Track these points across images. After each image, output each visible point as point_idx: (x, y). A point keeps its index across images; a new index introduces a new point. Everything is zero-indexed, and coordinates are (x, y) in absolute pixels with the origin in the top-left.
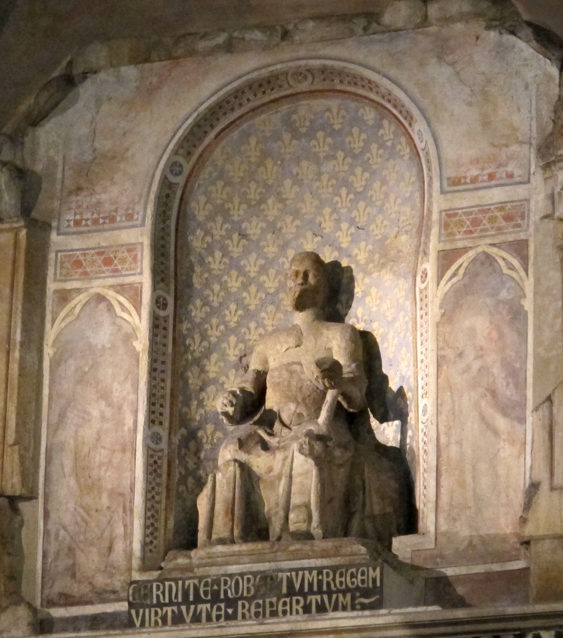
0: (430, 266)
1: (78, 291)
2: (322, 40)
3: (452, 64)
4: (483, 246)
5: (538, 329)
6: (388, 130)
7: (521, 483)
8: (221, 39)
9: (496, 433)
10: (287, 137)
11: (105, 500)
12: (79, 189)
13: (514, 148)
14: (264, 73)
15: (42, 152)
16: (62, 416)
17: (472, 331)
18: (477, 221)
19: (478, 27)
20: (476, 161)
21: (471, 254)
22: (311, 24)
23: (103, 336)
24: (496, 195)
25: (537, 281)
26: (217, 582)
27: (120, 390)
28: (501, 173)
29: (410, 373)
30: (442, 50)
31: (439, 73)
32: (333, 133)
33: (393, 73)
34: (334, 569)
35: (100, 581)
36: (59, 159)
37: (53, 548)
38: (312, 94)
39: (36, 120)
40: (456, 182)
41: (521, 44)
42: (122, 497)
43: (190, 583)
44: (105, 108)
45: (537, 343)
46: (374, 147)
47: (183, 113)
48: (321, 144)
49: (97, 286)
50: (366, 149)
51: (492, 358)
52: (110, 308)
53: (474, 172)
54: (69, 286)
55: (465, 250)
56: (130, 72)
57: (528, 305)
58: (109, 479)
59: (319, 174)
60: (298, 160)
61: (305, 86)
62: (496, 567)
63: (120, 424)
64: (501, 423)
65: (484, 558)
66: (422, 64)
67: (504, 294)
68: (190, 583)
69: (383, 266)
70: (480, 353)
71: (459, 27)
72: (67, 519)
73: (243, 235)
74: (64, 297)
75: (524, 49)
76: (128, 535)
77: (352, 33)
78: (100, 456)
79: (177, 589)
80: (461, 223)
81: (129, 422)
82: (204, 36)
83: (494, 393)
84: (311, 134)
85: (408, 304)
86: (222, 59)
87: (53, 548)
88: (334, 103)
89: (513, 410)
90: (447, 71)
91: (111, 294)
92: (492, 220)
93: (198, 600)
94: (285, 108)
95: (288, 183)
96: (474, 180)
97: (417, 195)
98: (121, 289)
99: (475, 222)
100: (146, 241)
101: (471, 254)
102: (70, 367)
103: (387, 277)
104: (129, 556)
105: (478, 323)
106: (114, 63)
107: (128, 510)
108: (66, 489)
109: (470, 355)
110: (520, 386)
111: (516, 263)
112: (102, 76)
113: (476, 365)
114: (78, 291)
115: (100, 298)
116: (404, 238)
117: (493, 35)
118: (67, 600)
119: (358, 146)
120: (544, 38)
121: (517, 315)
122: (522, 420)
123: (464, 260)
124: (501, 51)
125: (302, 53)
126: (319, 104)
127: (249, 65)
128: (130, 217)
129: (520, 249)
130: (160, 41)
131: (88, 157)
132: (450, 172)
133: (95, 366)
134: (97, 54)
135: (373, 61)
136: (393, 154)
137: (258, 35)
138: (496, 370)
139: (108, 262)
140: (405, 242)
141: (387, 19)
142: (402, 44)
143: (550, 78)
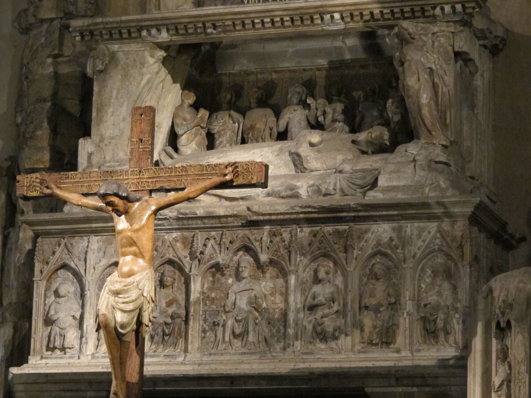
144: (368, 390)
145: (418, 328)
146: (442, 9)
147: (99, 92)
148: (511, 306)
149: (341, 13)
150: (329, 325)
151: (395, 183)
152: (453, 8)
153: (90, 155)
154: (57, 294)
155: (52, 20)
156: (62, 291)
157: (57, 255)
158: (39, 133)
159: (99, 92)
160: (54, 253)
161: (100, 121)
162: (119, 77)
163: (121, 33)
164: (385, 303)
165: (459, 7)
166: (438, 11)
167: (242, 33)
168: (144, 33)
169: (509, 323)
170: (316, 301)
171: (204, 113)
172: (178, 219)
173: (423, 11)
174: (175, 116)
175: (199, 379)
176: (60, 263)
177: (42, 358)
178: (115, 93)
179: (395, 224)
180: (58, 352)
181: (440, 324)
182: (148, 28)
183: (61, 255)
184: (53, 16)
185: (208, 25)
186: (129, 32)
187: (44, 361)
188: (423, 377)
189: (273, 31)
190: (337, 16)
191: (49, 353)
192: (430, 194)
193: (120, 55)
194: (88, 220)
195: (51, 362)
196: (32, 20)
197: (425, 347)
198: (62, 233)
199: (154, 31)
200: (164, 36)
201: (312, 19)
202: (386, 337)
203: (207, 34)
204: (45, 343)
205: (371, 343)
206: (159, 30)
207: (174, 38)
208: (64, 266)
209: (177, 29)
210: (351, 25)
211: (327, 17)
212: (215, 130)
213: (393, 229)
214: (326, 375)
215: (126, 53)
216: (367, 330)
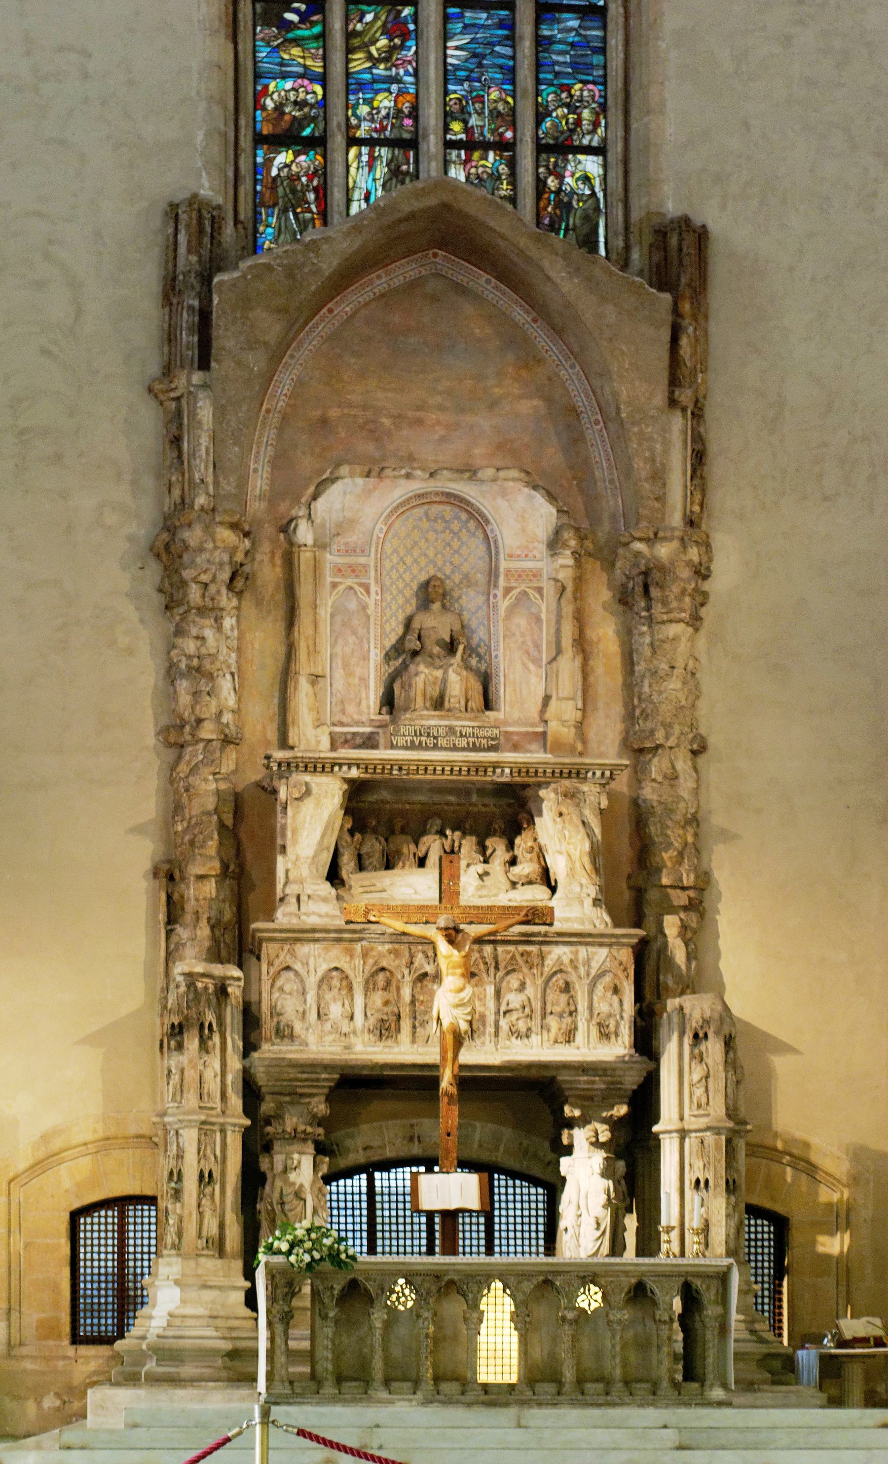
0: (500, 593)
1: (341, 583)
2: (450, 480)
3: (508, 500)
4: (523, 587)
5: (548, 627)
6: (472, 524)
7: (541, 694)
8: (403, 472)
9: (529, 671)
10: (425, 520)
11: (357, 681)
12: (338, 534)
13: (536, 544)
14: (422, 491)
15: (319, 514)
16: (336, 640)
17: (518, 626)
18: (520, 575)
19: (519, 485)
20: (518, 547)
21: (518, 590)
22: (445, 472)
23: (353, 605)
24: (529, 565)
25: (547, 607)
26: (429, 728)
27: (361, 631)
28: (530, 555)
29: (486, 638)
30: (504, 494)
31: (501, 502)
32: (446, 522)
33: (481, 500)
34: (479, 727)
35: (356, 717)
36: (327, 518)
37: (334, 700)
38: (439, 502)
39: (315, 497)
40: (511, 556)
41: (538, 496)
42: (364, 680)
43: (417, 728)
44: (348, 496)
45: (548, 634)
46: (464, 531)
47: (385, 505)
48: (440, 526)
49: (349, 582)
50: (460, 530)
51: (528, 638)
52: (356, 593)
53: (518, 552)
54: (336, 580)
55: (515, 588)
56: (360, 481)
57: (543, 616)
58: (358, 671)
59: (437, 540)
60: (427, 531)
61: (437, 499)
62: (531, 730)
63: (362, 647)
64: (532, 667)
65: (525, 724)
66: (495, 499)
67: (533, 610)
68: (417, 728)
69: (469, 586)
70: (523, 635)
71: (511, 483)
72: (340, 688)
73: (404, 563)
74: (334, 585)
75: (539, 499)
76: (367, 697)
77: (462, 479)
78: (354, 661)
79: (411, 729)
80: (513, 575)
81: (366, 646)
82: (394, 469)
83: (528, 654)
84: (435, 520)
85: (485, 607)
86: (403, 481)
87: (334, 700)
88: (448, 508)
89: (537, 661)
90: (506, 504)
91: (356, 587)
92: (527, 575)
93: (421, 734)
94: (426, 507)
95: (423, 541)
96: (519, 556)
97: (487, 557)
98: (361, 585)
99: (520, 576)
100: (372, 564)
101: (518, 590)
102: (338, 618)
103: (471, 593)
104: (369, 707)
105: (521, 621)
106: (352, 475)
107: (367, 687)
108: (339, 673)
109: (518, 634)
110: (540, 652)
111: (538, 596)
112: (346, 480)
113: (520, 640)
114: (341, 583)
115: (351, 588)
116: (479, 575)
117: (526, 490)
118: (342, 724)
119: (456, 529)
120: (551, 497)
121: (538, 620)
122: (541, 667)
123: (515, 592)
124: (531, 498)
125: (439, 484)
126: (441, 507)
127: (416, 486)
128: (363, 551)
129: (540, 590)
130: (374, 469)
131: (341, 519)
132: (507, 551)
133: (350, 619)
134: (344, 470)
135: (472, 493)
136: (474, 535)
137: (419, 473)
138: (530, 643)
139: (354, 571)
140: (481, 578)
141: (480, 475)
142: (485, 488)
143: (551, 514)
144: (559, 1078)
145: (594, 1031)
146: (594, 774)
147: (294, 816)
148: (708, 1022)
149: (511, 768)
150: (522, 1026)
151: (568, 915)
152: (603, 774)
153: (287, 871)
154: (281, 989)
155: (211, 741)
156: (287, 988)
157: (282, 958)
158: (210, 843)
159: (294, 816)
160: (277, 956)
161: (295, 842)
162: (312, 805)
163: (315, 767)
164: (567, 1010)
165: (608, 773)
166: (590, 774)
167: (422, 777)
168: (336, 768)
169: (706, 1036)
170: (511, 1006)
171: (358, 836)
172: (392, 934)
173: (578, 773)
174: (339, 838)
175: (414, 1066)
176: (285, 965)
177: (273, 1044)
178: (308, 818)
179: (573, 948)
180: (286, 1040)
181: (612, 1028)
182: (340, 765)
183: (284, 958)
184: (214, 737)
185: (396, 767)
186: (323, 767)
187: (275, 1047)
188: (605, 1070)
189: (451, 778)
190: (507, 771)
191: (278, 1040)
192: (601, 928)
193: (313, 785)
194: (314, 930)
195: (284, 1048)
196: (188, 737)
197: (600, 1046)
198: (285, 940)
199: (345, 768)
200: (354, 773)
201: (485, 771)
202: (569, 1036)
203: (391, 774)
204: (273, 1032)
205: (556, 1042)
206: (349, 768)
207: (362, 776)
208: (288, 968)
209: (366, 768)
210: (518, 779)
211: (499, 771)
212: (364, 850)
213: (572, 952)
214: (530, 1066)
215: (318, 784)
216: (554, 1030)
